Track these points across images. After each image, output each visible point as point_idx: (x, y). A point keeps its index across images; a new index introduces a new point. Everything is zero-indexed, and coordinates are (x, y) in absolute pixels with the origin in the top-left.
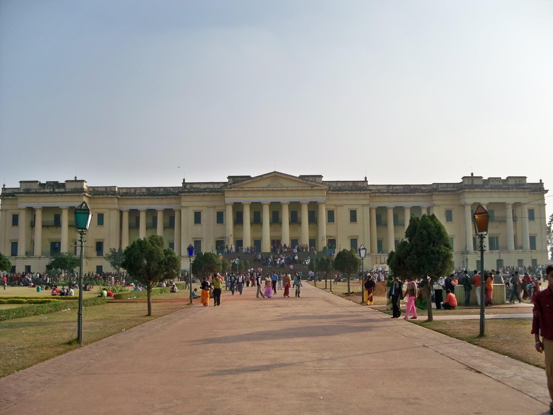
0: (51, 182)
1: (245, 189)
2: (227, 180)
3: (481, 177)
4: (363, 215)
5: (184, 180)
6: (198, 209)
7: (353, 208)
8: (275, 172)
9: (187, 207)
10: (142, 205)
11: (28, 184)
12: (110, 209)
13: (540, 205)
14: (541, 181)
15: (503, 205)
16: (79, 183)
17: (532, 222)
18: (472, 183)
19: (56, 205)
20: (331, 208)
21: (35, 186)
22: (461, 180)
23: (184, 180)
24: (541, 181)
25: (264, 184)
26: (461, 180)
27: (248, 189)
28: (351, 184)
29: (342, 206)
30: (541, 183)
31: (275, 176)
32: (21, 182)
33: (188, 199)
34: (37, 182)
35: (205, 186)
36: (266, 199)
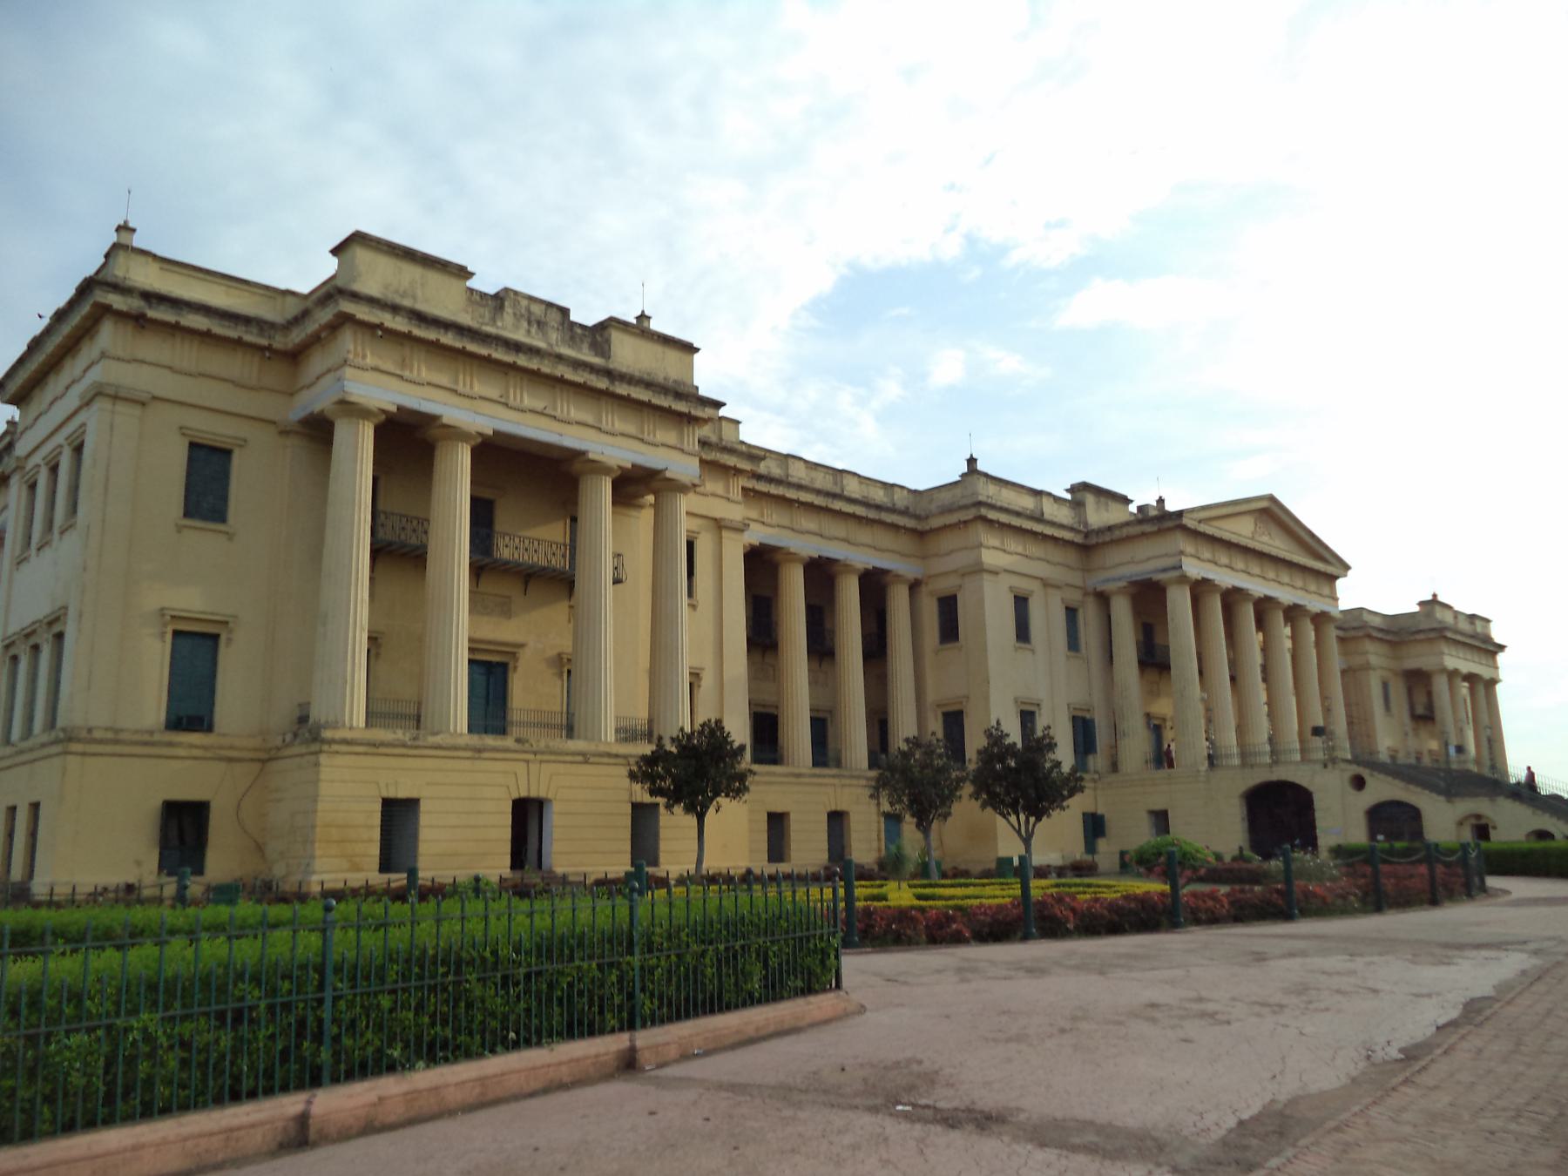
0: (531, 299)
2: (1068, 496)
5: (972, 461)
6: (1024, 585)
8: (1272, 498)
9: (994, 573)
10: (803, 540)
11: (412, 272)
12: (719, 525)
16: (673, 355)
19: (571, 438)
21: (442, 300)
22: (1417, 609)
23: (972, 461)
26: (1417, 609)
31: (1270, 512)
33: (990, 539)
34: (463, 273)
35: (1028, 503)
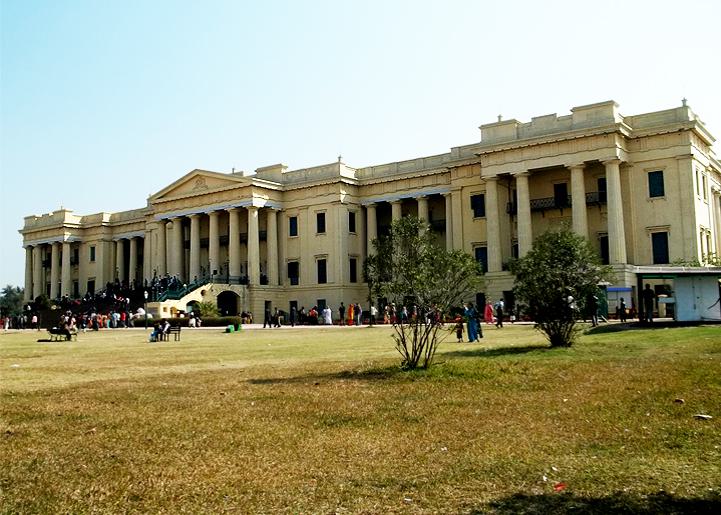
1: (170, 199)
3: (514, 121)
4: (337, 220)
7: (320, 209)
13: (676, 159)
14: (684, 101)
15: (563, 171)
17: (658, 201)
18: (502, 138)
20: (293, 213)
24: (684, 101)
25: (189, 190)
27: (174, 198)
28: (319, 171)
29: (307, 207)
30: (685, 107)
31: (197, 177)
32: (26, 218)
36: (191, 211)
